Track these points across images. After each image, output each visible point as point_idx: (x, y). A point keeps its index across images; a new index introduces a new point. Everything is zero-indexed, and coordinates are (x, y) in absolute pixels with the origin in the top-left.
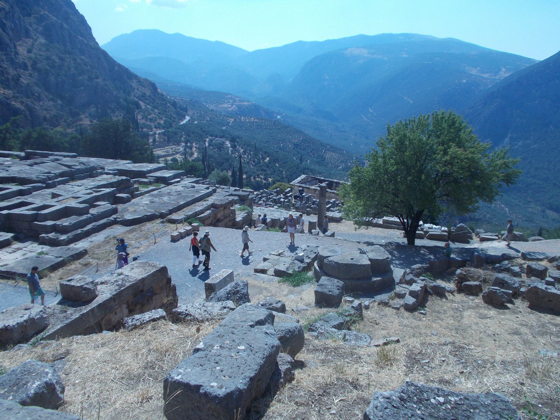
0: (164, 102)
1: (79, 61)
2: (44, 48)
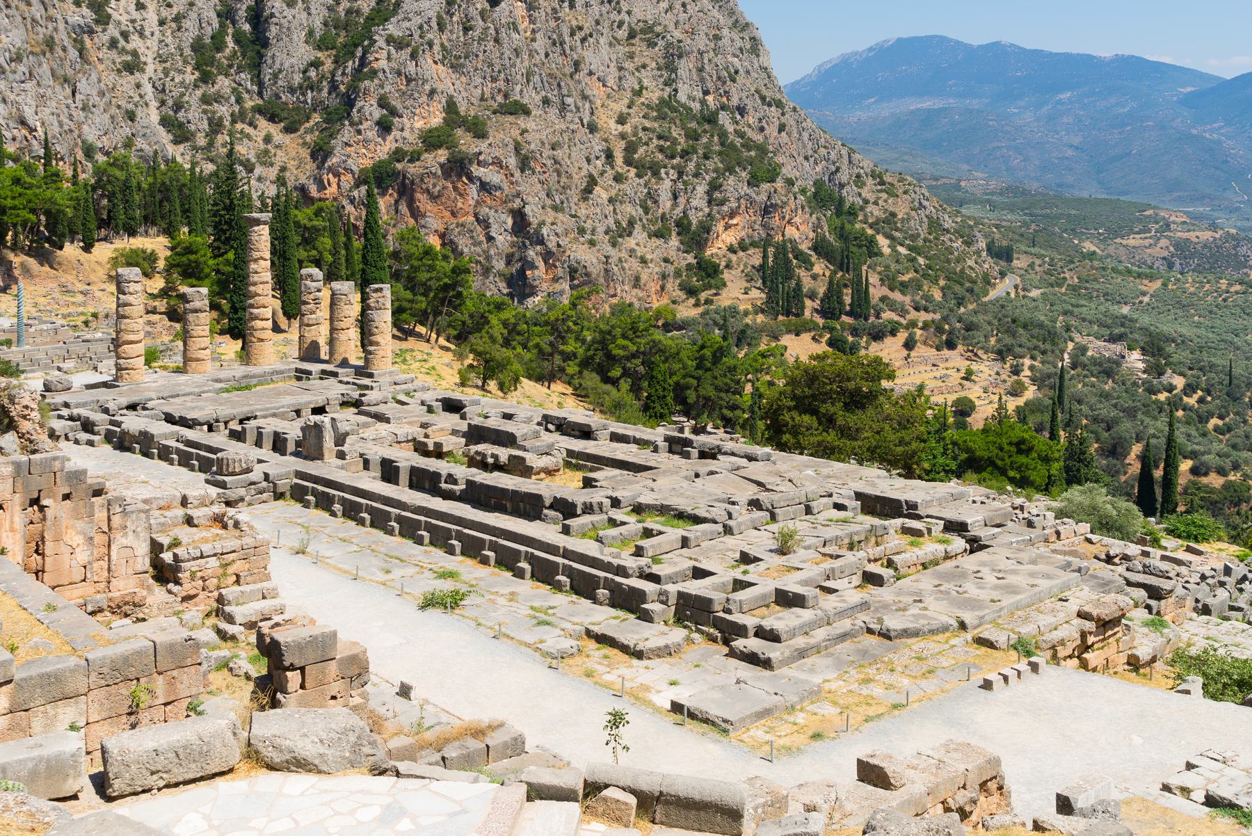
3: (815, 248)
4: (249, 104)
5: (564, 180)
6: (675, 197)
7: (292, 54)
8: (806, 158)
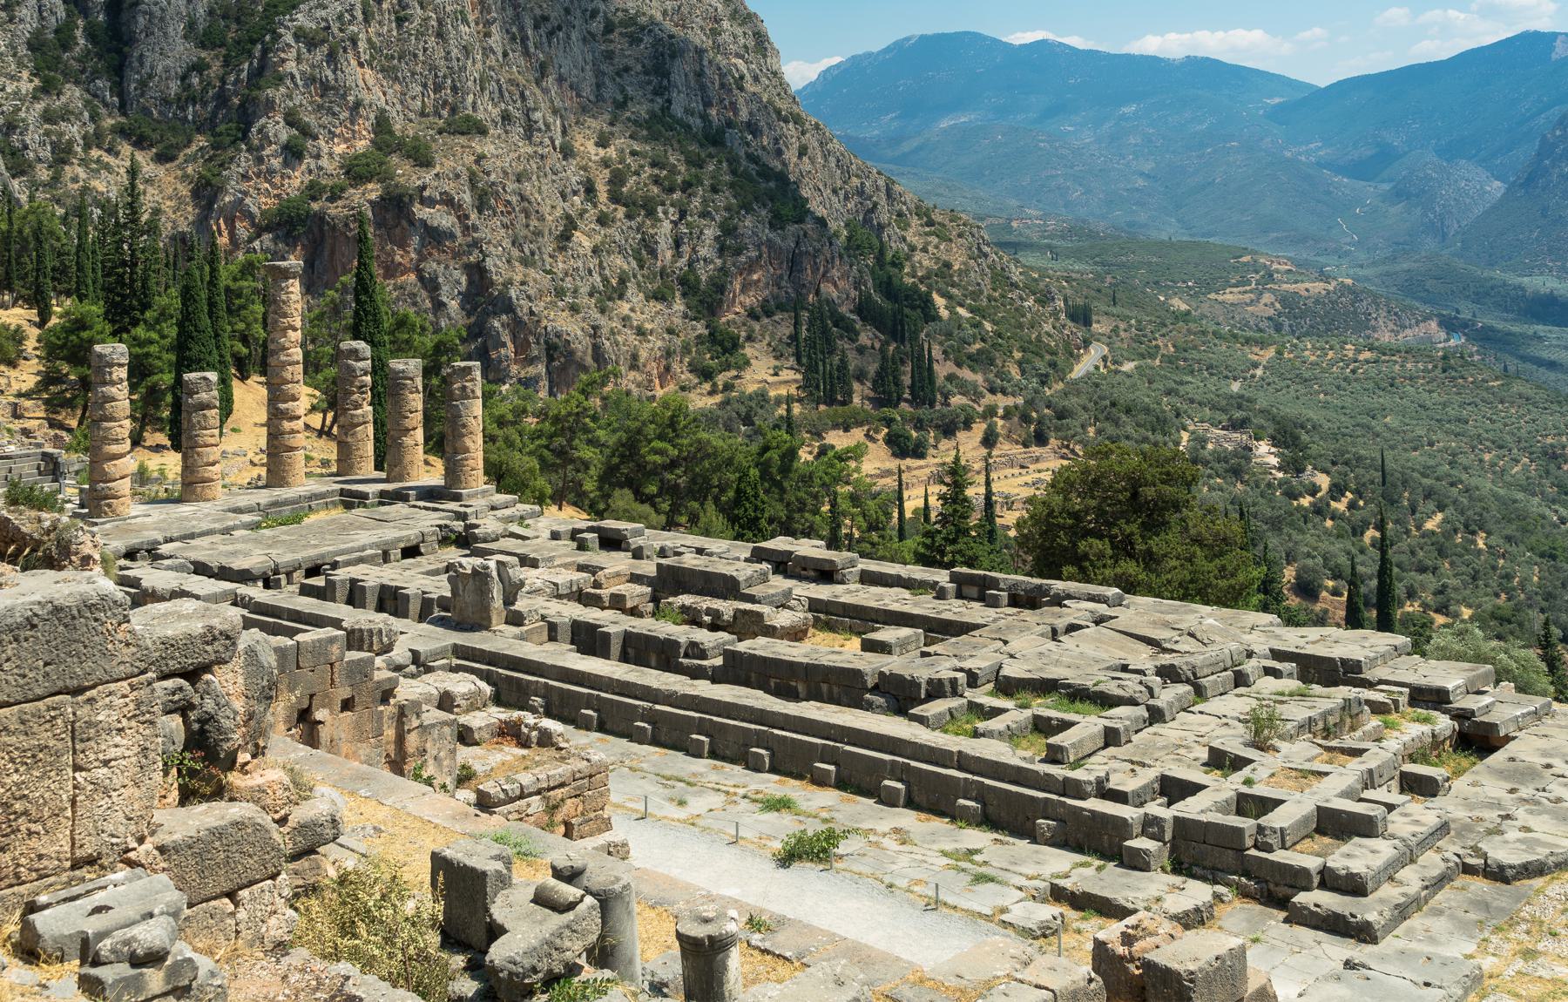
0: (1013, 295)
2: (645, 132)
3: (859, 310)
4: (109, 122)
5: (534, 223)
6: (678, 243)
7: (168, 55)
8: (835, 191)
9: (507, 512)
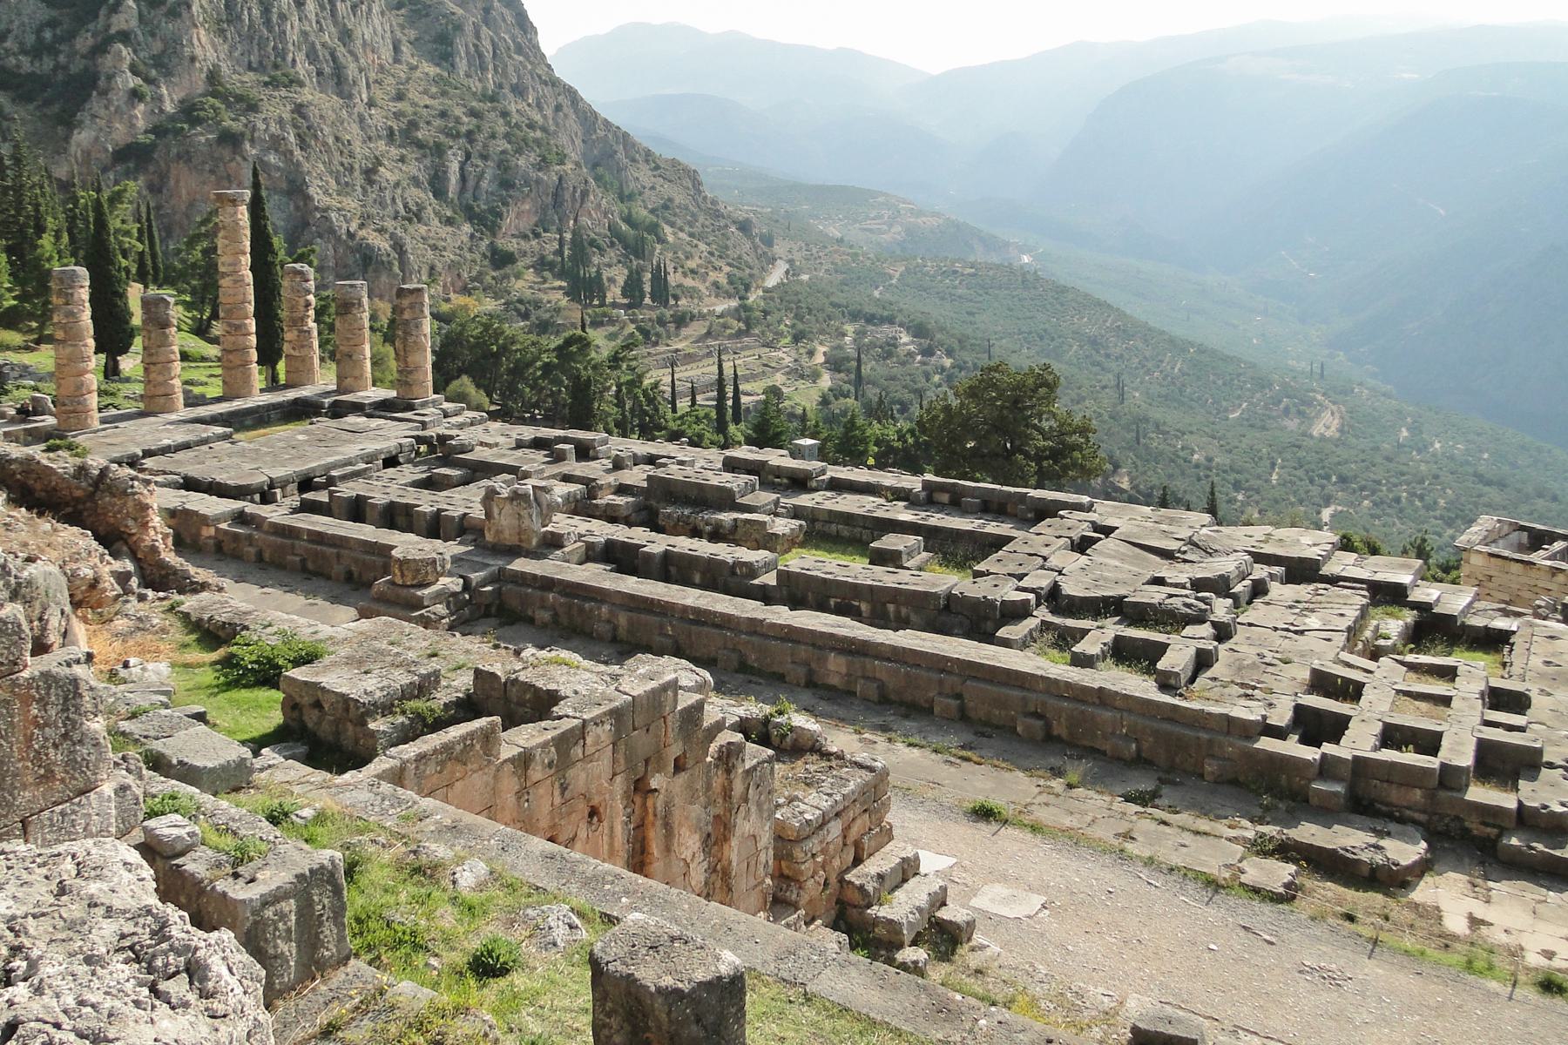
1: (515, 118)
2: (434, 90)
6: (463, 178)
9: (459, 419)
